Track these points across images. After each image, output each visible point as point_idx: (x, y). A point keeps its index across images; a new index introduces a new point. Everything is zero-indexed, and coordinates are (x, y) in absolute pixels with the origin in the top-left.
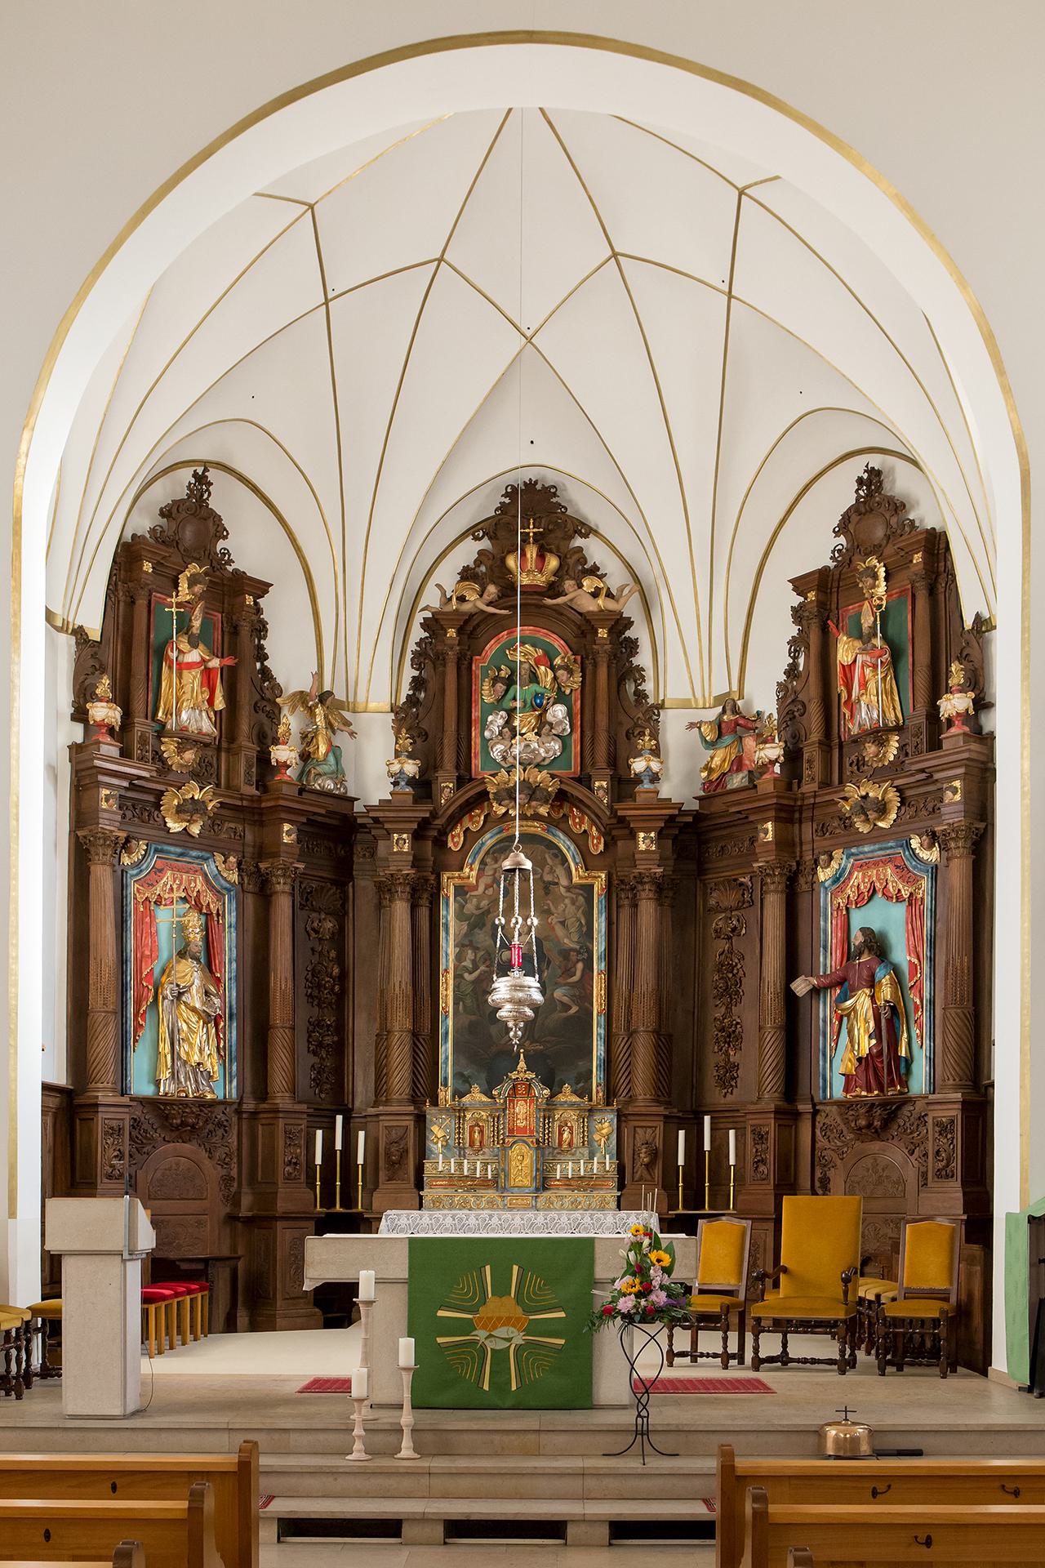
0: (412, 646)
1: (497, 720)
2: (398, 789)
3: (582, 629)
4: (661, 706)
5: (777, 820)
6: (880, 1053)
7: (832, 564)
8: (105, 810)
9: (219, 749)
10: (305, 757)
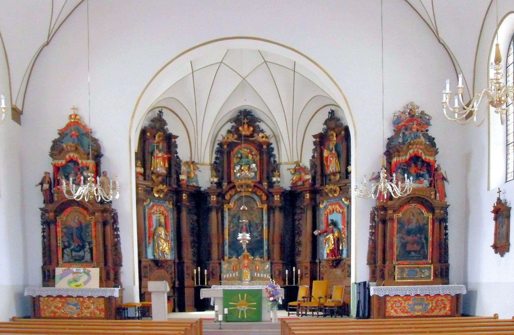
0: (215, 149)
1: (238, 168)
2: (212, 185)
3: (259, 146)
4: (280, 164)
5: (310, 193)
6: (335, 248)
7: (323, 132)
8: (140, 193)
9: (167, 177)
10: (188, 177)
